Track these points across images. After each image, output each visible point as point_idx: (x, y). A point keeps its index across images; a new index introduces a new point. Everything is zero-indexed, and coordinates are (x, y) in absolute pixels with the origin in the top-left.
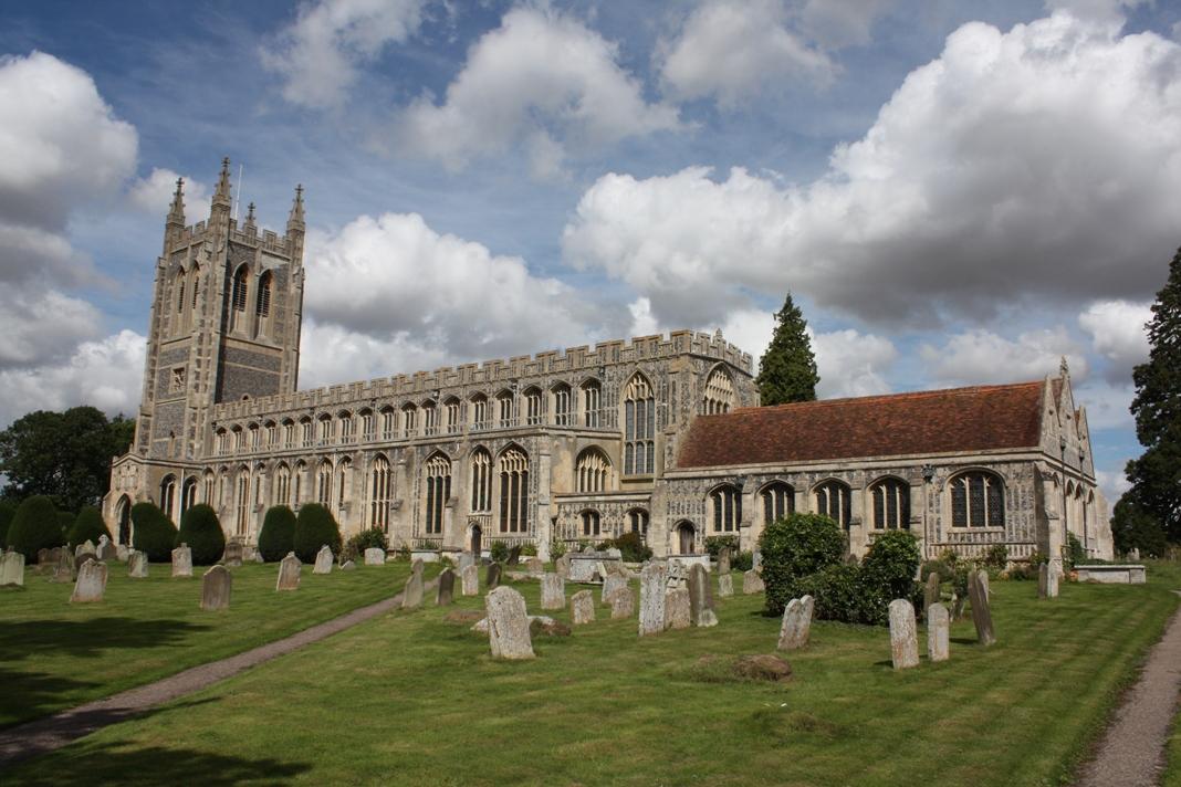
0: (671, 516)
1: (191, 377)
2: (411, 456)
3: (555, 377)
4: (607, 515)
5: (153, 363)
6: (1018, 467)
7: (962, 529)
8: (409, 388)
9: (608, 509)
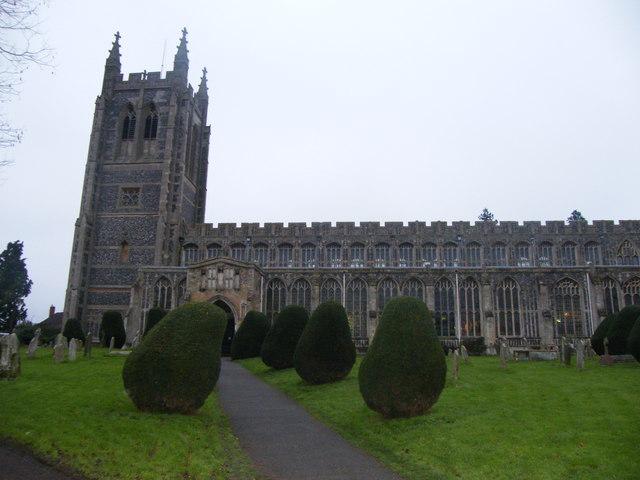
5: (96, 178)
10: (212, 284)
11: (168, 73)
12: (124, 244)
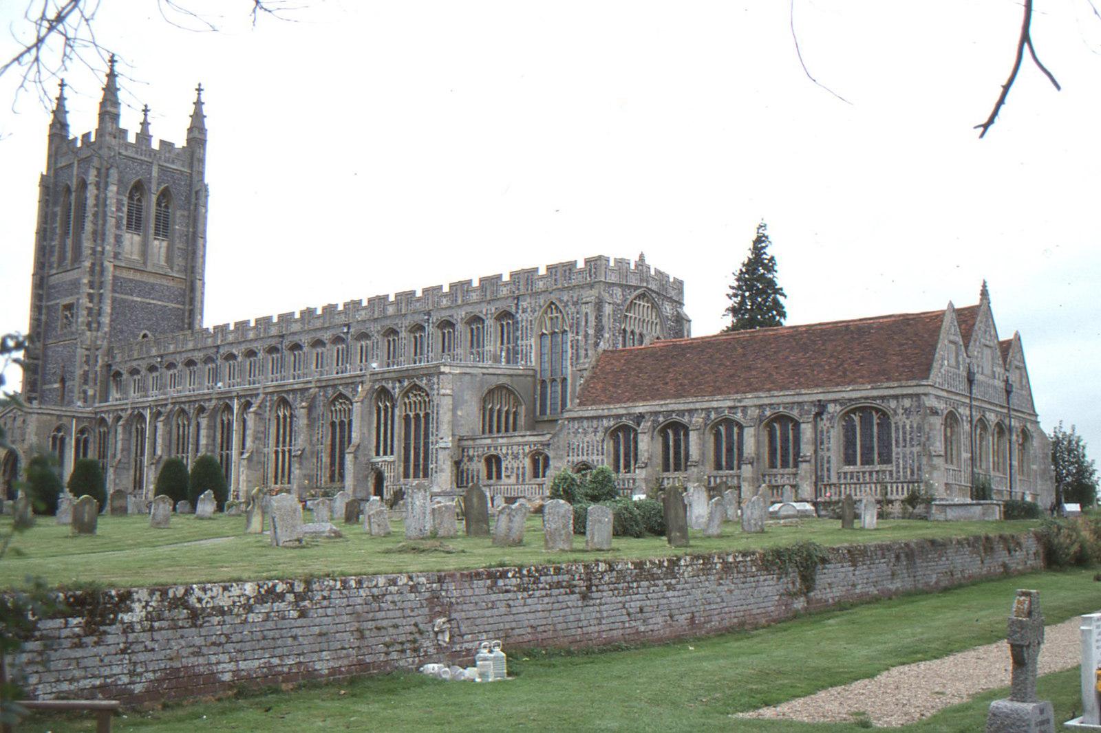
0: (570, 458)
1: (82, 318)
2: (314, 398)
3: (469, 309)
4: (510, 457)
6: (907, 403)
7: (851, 468)
8: (318, 324)
9: (510, 452)
12: (63, 381)
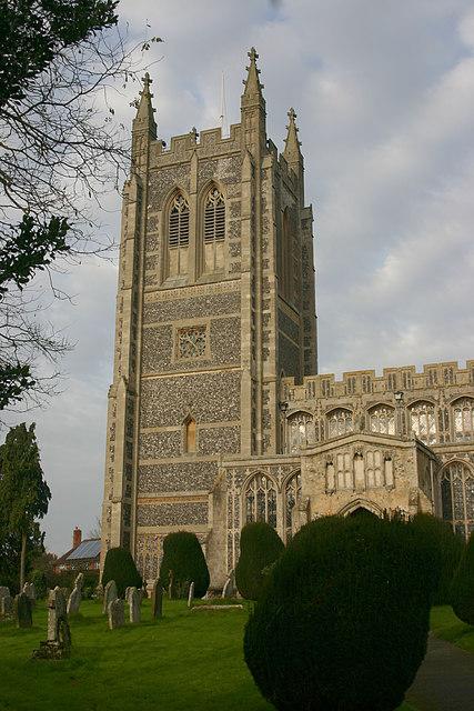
10: (345, 481)
11: (234, 128)
